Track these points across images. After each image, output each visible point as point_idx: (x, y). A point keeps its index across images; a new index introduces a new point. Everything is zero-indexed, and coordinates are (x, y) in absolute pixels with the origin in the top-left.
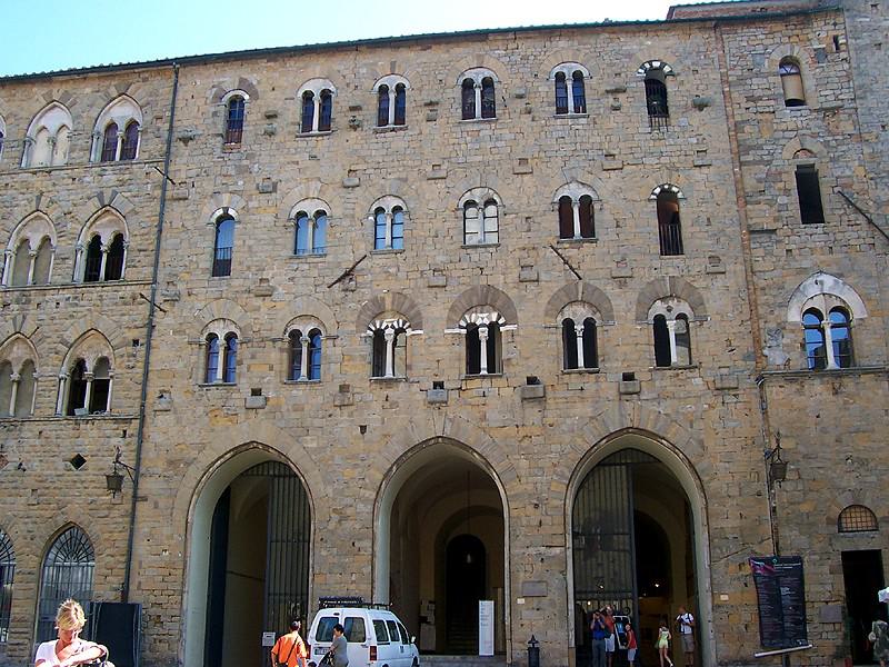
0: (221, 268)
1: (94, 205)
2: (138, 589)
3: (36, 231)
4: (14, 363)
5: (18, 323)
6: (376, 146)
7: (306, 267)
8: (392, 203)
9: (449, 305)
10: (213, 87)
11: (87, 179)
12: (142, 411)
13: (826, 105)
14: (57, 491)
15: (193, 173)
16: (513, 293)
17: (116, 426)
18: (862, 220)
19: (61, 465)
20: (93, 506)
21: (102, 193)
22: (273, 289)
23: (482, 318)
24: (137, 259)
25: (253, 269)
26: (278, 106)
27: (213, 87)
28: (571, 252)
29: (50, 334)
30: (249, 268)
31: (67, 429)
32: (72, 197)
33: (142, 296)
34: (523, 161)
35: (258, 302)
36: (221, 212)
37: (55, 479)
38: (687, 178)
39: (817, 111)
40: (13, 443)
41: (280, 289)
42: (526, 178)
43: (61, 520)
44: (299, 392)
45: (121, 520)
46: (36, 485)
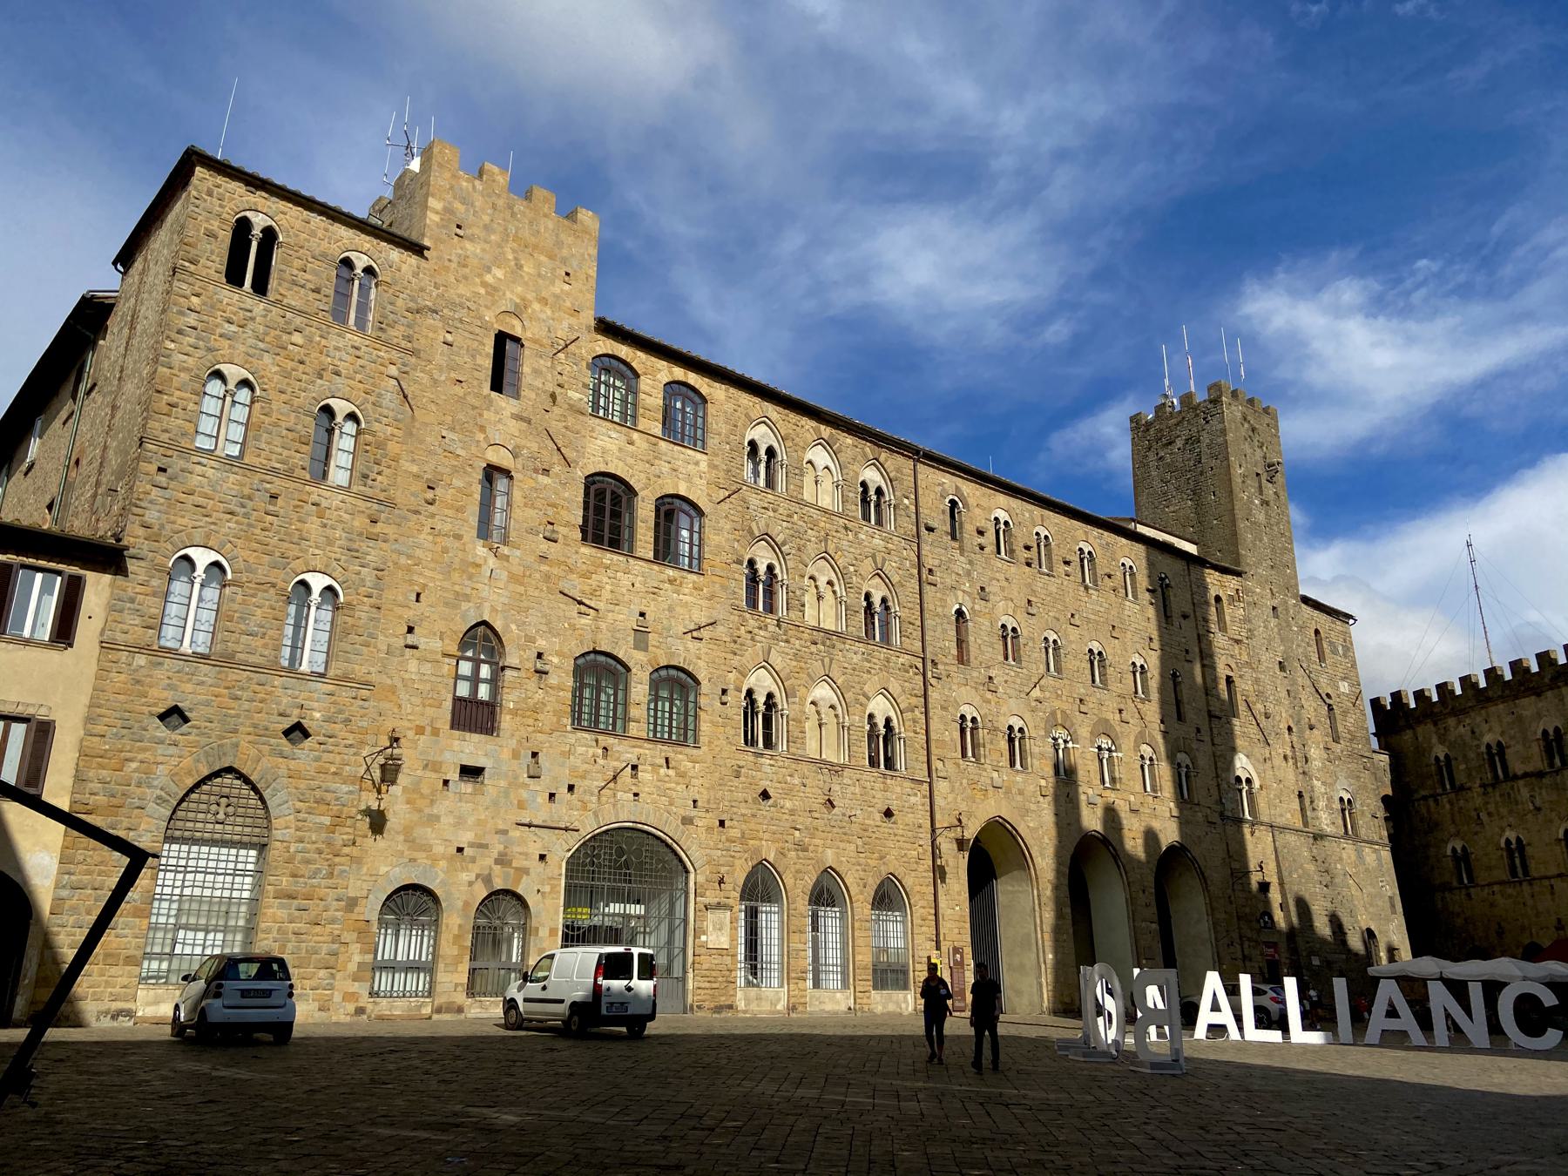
0: (962, 658)
1: (867, 566)
2: (945, 939)
3: (820, 570)
4: (821, 703)
5: (827, 668)
6: (1041, 585)
7: (1013, 674)
8: (1052, 637)
9: (1090, 729)
10: (939, 484)
11: (863, 537)
12: (930, 775)
13: (1236, 637)
14: (877, 841)
15: (937, 562)
16: (1118, 729)
17: (913, 786)
18: (1254, 722)
19: (878, 816)
20: (904, 859)
21: (874, 554)
22: (997, 687)
23: (1105, 743)
24: (909, 631)
25: (984, 665)
26: (982, 524)
27: (939, 484)
28: (1140, 706)
29: (854, 684)
30: (981, 663)
31: (872, 777)
32: (852, 550)
33: (917, 668)
34: (1113, 627)
35: (989, 695)
36: (957, 606)
37: (875, 829)
38: (1183, 667)
39: (1233, 639)
40: (836, 788)
41: (1001, 689)
42: (1117, 641)
43: (884, 871)
44: (1019, 778)
45: (926, 874)
46: (862, 833)
